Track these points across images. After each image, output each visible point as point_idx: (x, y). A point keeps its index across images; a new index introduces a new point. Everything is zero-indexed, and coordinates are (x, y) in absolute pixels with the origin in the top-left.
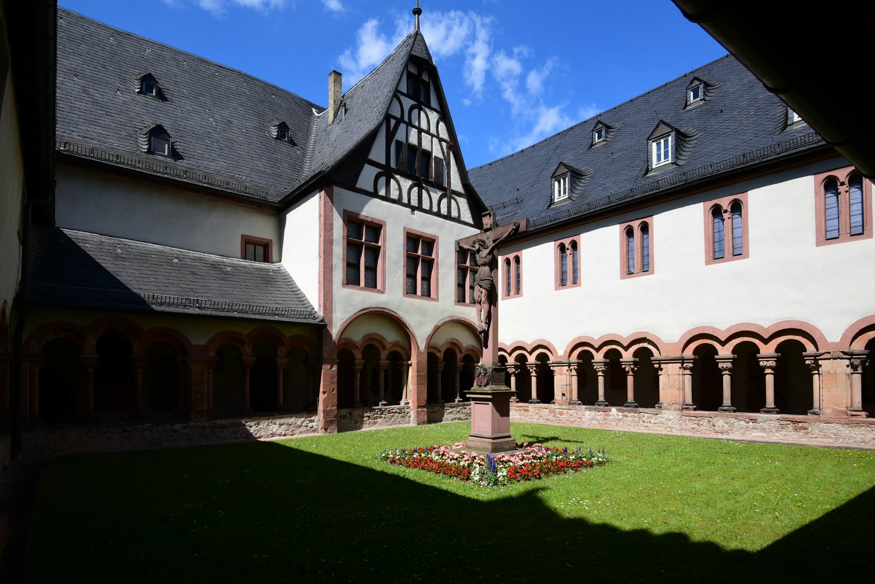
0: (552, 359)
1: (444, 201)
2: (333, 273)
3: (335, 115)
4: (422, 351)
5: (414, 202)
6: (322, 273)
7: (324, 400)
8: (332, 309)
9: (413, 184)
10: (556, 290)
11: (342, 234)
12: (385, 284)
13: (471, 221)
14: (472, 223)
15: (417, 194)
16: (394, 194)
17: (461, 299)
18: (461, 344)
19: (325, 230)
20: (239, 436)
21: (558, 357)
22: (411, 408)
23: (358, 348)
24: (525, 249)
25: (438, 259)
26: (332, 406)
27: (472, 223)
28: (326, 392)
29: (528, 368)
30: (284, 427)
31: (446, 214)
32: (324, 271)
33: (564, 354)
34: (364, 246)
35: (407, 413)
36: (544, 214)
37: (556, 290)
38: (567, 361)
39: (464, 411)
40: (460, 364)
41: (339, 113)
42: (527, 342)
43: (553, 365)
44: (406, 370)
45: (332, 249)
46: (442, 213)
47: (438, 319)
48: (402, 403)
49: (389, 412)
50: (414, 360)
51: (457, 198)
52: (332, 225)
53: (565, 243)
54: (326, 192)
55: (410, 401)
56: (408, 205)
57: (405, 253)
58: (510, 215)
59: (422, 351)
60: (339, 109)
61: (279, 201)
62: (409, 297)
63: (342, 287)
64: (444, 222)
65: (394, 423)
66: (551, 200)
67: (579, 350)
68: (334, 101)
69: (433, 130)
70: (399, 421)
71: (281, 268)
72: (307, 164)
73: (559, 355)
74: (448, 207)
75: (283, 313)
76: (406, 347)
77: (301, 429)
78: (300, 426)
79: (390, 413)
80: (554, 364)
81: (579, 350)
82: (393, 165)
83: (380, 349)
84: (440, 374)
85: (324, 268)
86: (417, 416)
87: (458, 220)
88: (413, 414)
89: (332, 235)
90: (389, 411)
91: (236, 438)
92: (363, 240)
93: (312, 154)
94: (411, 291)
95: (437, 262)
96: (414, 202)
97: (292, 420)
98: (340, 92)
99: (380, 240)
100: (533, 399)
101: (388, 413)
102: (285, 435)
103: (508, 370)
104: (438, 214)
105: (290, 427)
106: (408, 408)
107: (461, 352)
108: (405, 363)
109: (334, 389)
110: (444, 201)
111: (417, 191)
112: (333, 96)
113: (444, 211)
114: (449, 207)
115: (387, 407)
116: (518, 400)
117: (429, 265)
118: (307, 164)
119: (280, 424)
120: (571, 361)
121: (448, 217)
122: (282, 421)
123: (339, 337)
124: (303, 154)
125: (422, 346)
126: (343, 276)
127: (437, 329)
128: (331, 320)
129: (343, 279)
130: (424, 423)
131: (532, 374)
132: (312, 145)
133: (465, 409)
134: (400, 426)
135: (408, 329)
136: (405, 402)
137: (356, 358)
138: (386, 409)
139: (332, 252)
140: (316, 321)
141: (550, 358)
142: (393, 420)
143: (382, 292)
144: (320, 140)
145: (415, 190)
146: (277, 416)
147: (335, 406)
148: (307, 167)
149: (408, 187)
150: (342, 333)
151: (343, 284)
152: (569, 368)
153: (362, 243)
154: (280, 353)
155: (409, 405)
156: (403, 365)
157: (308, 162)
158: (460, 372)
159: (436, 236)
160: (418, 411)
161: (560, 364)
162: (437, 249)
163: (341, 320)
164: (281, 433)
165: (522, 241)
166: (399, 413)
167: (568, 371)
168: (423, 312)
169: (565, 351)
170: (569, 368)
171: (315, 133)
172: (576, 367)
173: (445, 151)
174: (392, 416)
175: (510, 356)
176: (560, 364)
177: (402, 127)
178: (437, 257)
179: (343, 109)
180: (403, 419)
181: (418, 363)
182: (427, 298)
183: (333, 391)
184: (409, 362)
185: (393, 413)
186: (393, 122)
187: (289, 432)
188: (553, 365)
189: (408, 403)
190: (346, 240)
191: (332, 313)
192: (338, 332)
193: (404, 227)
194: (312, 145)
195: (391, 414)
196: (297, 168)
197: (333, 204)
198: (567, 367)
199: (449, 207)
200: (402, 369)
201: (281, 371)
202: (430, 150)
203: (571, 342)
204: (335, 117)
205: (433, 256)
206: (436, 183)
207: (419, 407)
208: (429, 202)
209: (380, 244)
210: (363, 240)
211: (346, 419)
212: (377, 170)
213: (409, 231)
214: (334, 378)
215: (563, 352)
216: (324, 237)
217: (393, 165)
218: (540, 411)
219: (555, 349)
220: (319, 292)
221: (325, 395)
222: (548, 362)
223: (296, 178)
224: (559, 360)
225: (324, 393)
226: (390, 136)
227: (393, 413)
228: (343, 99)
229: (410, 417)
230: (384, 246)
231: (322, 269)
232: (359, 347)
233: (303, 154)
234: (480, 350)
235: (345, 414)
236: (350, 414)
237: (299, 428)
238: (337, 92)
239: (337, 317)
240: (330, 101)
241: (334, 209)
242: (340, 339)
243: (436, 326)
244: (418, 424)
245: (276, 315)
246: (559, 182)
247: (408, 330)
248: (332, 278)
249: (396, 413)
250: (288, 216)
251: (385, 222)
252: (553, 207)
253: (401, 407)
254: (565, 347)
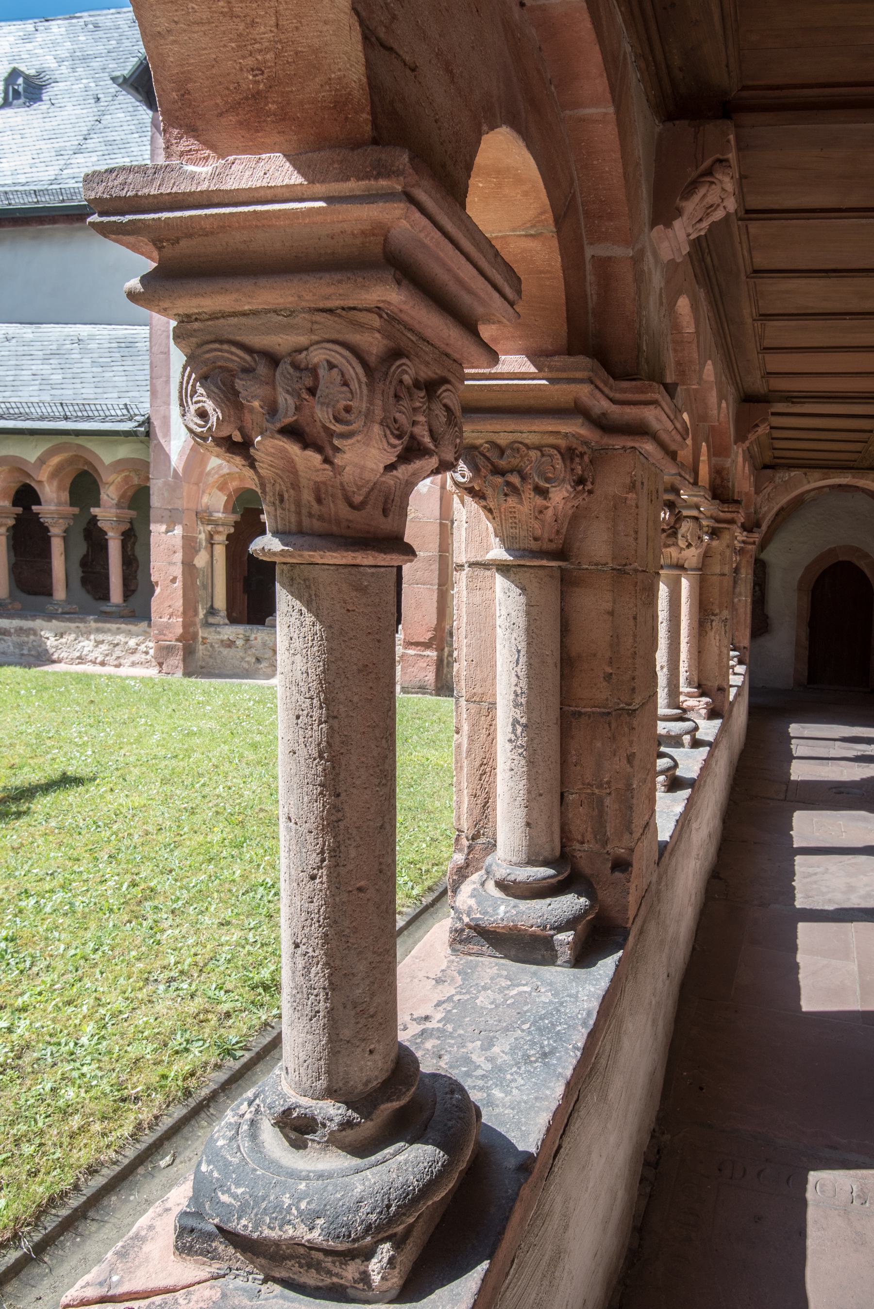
20: (25, 652)
30: (104, 647)
77: (136, 658)
78: (134, 652)
91: (23, 655)
97: (121, 638)
102: (103, 664)
105: (116, 649)
119: (96, 641)
122: (100, 637)
146: (93, 625)
164: (96, 658)
187: (111, 660)
237: (132, 653)
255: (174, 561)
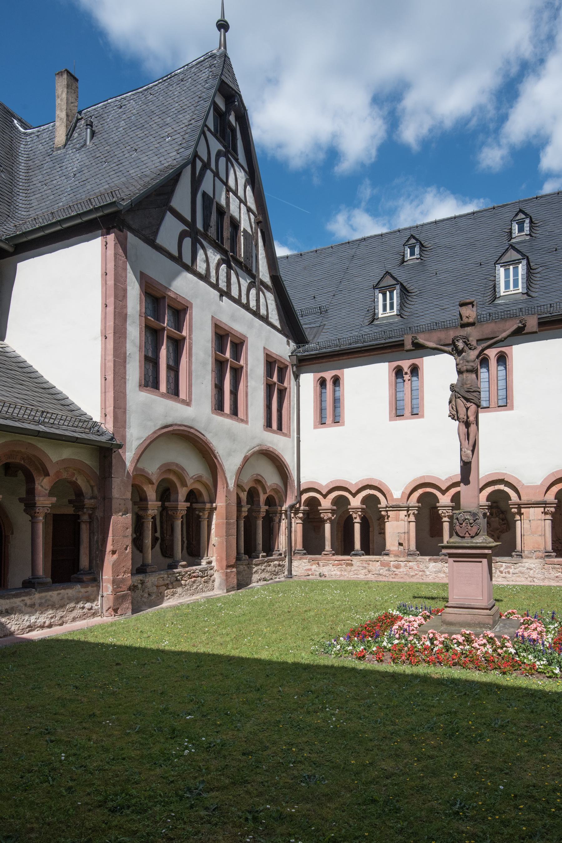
0: (383, 502)
1: (253, 292)
2: (128, 366)
3: (69, 136)
4: (232, 490)
5: (223, 285)
6: (110, 365)
7: (113, 565)
8: (125, 422)
9: (222, 259)
10: (390, 420)
11: (139, 309)
12: (192, 392)
13: (277, 324)
14: (279, 327)
15: (226, 275)
16: (201, 267)
17: (269, 424)
18: (266, 482)
19: (116, 297)
21: (393, 499)
22: (215, 568)
23: (151, 483)
24: (348, 367)
25: (247, 368)
26: (125, 573)
27: (279, 327)
28: (116, 551)
29: (351, 513)
31: (255, 309)
32: (114, 361)
33: (402, 496)
34: (166, 332)
35: (211, 577)
36: (368, 330)
37: (390, 420)
38: (405, 505)
39: (269, 569)
40: (264, 508)
41: (76, 135)
42: (351, 481)
43: (387, 509)
44: (206, 516)
45: (126, 329)
46: (251, 307)
47: (248, 448)
48: (204, 562)
49: (190, 577)
50: (220, 503)
51: (265, 291)
52: (125, 290)
53: (403, 366)
54: (117, 237)
55: (213, 559)
56: (215, 286)
57: (214, 353)
58: (314, 325)
59: (232, 490)
60: (74, 130)
61: (6, 239)
62: (217, 415)
63: (138, 388)
64: (253, 319)
65: (196, 592)
66: (375, 314)
67: (420, 491)
68: (67, 116)
69: (241, 193)
70: (202, 589)
71: (7, 349)
72: (21, 198)
73: (395, 497)
74: (256, 300)
75: (52, 421)
76: (207, 482)
79: (191, 578)
80: (389, 508)
81: (420, 491)
82: (199, 225)
83: (178, 485)
84: (243, 522)
85: (115, 356)
86: (227, 579)
87: (265, 319)
88: (218, 577)
89: (125, 307)
90: (190, 575)
92: (165, 325)
93: (26, 185)
94: (219, 407)
95: (247, 372)
96: (223, 285)
98: (76, 104)
99: (185, 327)
100: (357, 550)
101: (189, 578)
103: (322, 515)
104: (246, 307)
106: (211, 569)
107: (265, 493)
108: (208, 506)
109: (127, 546)
110: (253, 292)
111: (225, 270)
112: (64, 107)
113: (253, 304)
114: (258, 301)
115: (187, 569)
116: (333, 552)
117: (237, 372)
118: (21, 198)
120: (410, 505)
121: (256, 314)
123: (134, 465)
124: (11, 181)
125: (231, 483)
126: (140, 373)
127: (246, 460)
128: (124, 437)
129: (140, 377)
130: (233, 589)
131: (355, 521)
132: (23, 171)
133: (270, 566)
134: (204, 595)
135: (216, 458)
136: (208, 560)
137: (148, 498)
138: (186, 572)
139: (126, 333)
140: (103, 439)
141: (381, 501)
142: (195, 587)
143: (188, 403)
144: (40, 167)
145: (224, 267)
147: (128, 573)
148: (21, 201)
149: (216, 261)
150: (138, 460)
151: (140, 386)
152: (408, 512)
153: (164, 329)
154: (40, 488)
155: (213, 565)
156: (204, 509)
157: (21, 194)
158: (263, 518)
159: (245, 337)
160: (227, 573)
161: (397, 508)
162: (247, 354)
163: (138, 439)
165: (344, 358)
166: (202, 577)
167: (406, 516)
168: (232, 437)
169: (403, 493)
170: (408, 512)
171: (25, 156)
172: (416, 512)
173: (254, 226)
174: (194, 582)
175: (325, 498)
176: (397, 508)
177: (209, 175)
178: (247, 365)
179: (89, 130)
180: (206, 584)
181: (228, 506)
182: (234, 417)
183: (126, 549)
184: (214, 505)
185: (194, 577)
186: (199, 165)
188: (387, 509)
189: (210, 563)
190: (144, 318)
191: (125, 428)
192: (134, 458)
193: (212, 316)
194: (23, 171)
195: (193, 579)
196: (7, 199)
197: (126, 258)
198: (406, 512)
199: (258, 301)
200: (201, 514)
201: (41, 518)
202: (238, 219)
203: (411, 482)
204: (68, 140)
205: (242, 363)
206: (246, 267)
207: (228, 567)
208: (238, 288)
209: (184, 333)
210: (165, 325)
211: (137, 591)
212: (183, 227)
213: (218, 323)
214: (127, 529)
215: (400, 495)
216: (115, 308)
217: (199, 225)
218: (369, 564)
219: (389, 491)
220: (104, 392)
221: (115, 556)
222: (379, 506)
223: (8, 214)
224: (394, 504)
225: (114, 552)
226: (196, 183)
227: (194, 577)
228: (80, 117)
229: (214, 581)
230: (190, 339)
231: (110, 357)
232: (154, 481)
233: (11, 181)
234: (284, 489)
235: (136, 584)
236: (143, 583)
238: (72, 103)
239: (132, 435)
240: (58, 112)
241: (128, 267)
242: (136, 468)
243: (245, 457)
244: (228, 591)
245: (39, 423)
246: (384, 295)
247: (215, 460)
248: (125, 373)
249: (198, 577)
250: (20, 266)
251: (191, 304)
252: (376, 322)
253: (204, 568)
254: (403, 489)
255: (127, 534)
